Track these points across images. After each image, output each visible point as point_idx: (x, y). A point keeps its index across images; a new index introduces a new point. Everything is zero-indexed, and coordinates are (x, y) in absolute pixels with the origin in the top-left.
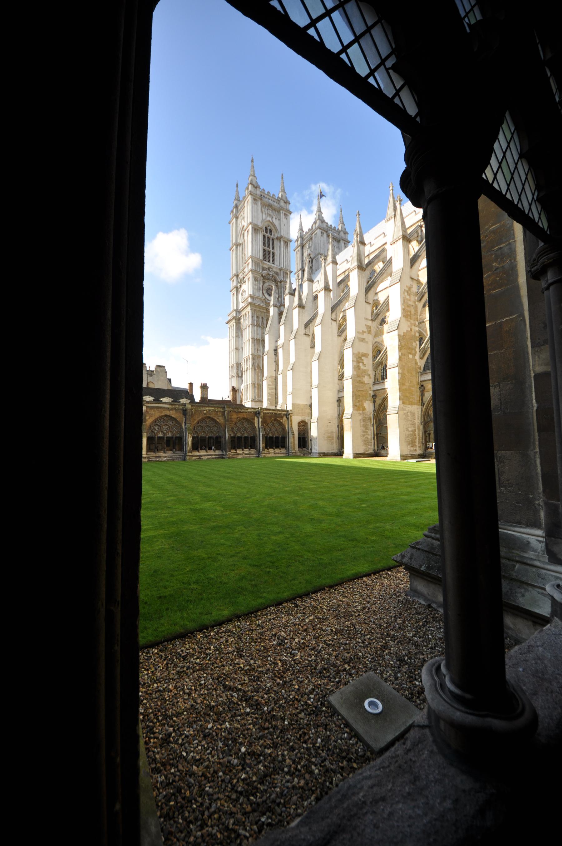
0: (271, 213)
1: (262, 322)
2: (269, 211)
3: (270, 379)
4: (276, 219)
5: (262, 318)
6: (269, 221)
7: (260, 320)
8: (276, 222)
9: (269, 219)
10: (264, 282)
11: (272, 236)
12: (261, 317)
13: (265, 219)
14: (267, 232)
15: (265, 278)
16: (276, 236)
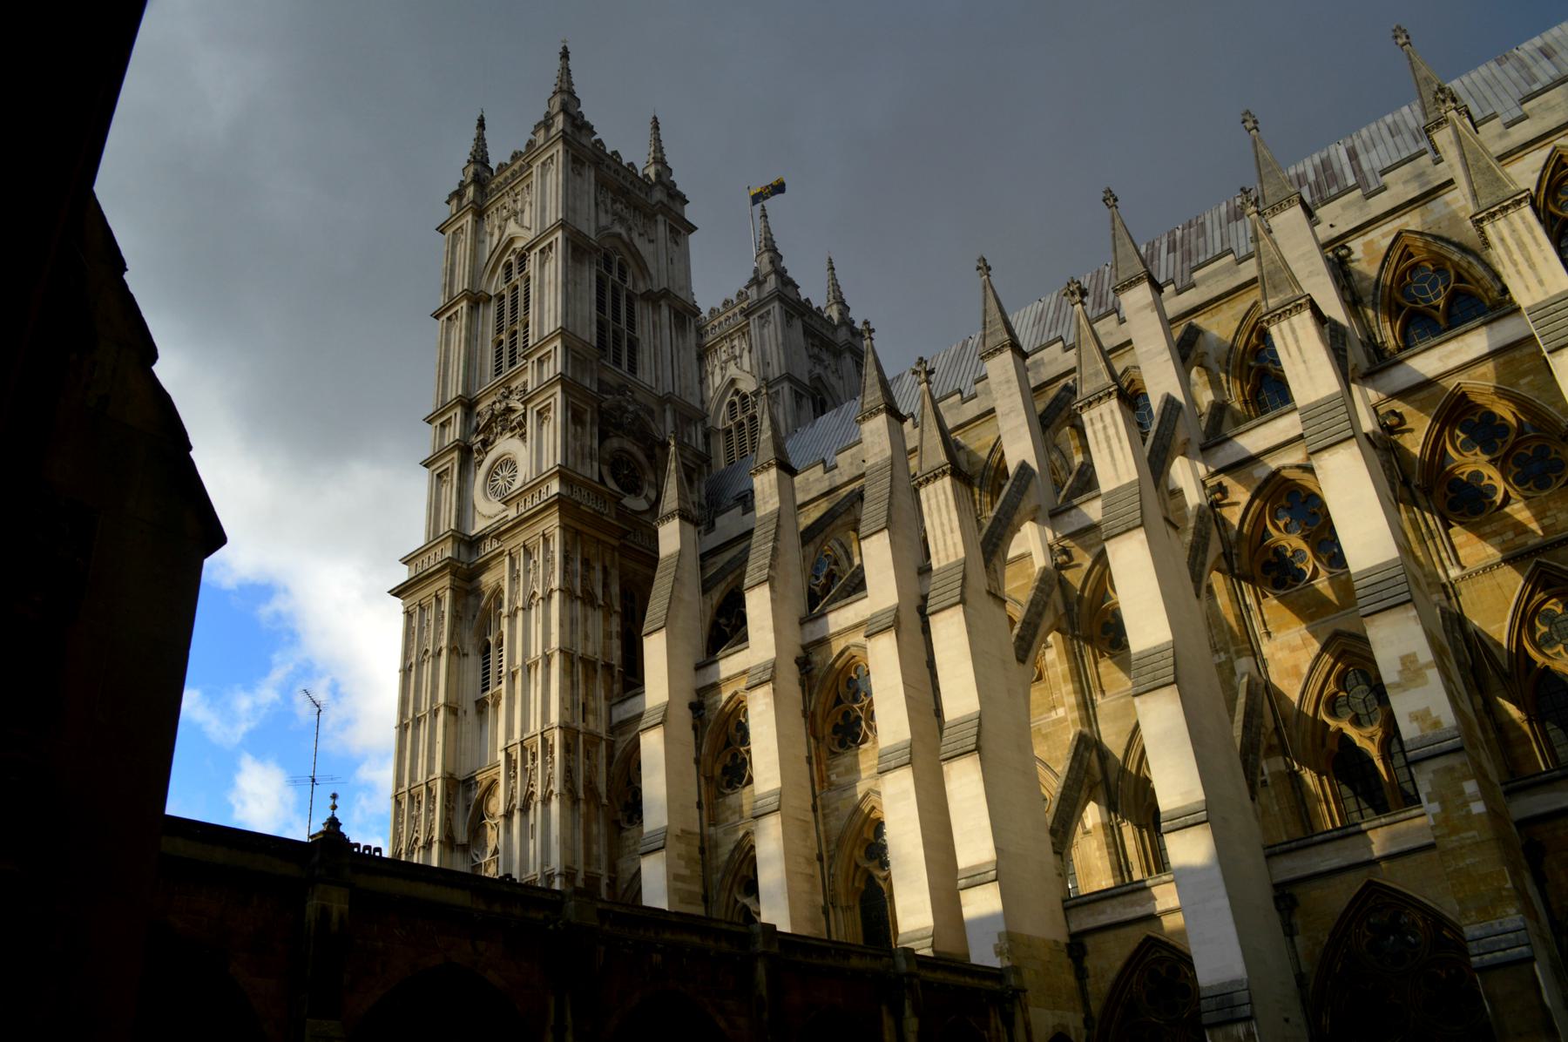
0: (626, 214)
1: (605, 586)
2: (618, 206)
3: (681, 848)
4: (640, 235)
5: (605, 570)
6: (619, 236)
7: (598, 575)
8: (641, 245)
9: (618, 229)
10: (603, 437)
11: (629, 284)
12: (598, 567)
13: (606, 228)
14: (609, 269)
15: (608, 424)
16: (642, 287)
